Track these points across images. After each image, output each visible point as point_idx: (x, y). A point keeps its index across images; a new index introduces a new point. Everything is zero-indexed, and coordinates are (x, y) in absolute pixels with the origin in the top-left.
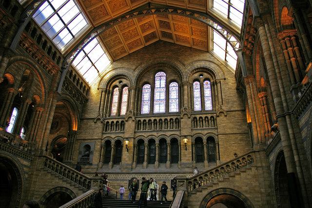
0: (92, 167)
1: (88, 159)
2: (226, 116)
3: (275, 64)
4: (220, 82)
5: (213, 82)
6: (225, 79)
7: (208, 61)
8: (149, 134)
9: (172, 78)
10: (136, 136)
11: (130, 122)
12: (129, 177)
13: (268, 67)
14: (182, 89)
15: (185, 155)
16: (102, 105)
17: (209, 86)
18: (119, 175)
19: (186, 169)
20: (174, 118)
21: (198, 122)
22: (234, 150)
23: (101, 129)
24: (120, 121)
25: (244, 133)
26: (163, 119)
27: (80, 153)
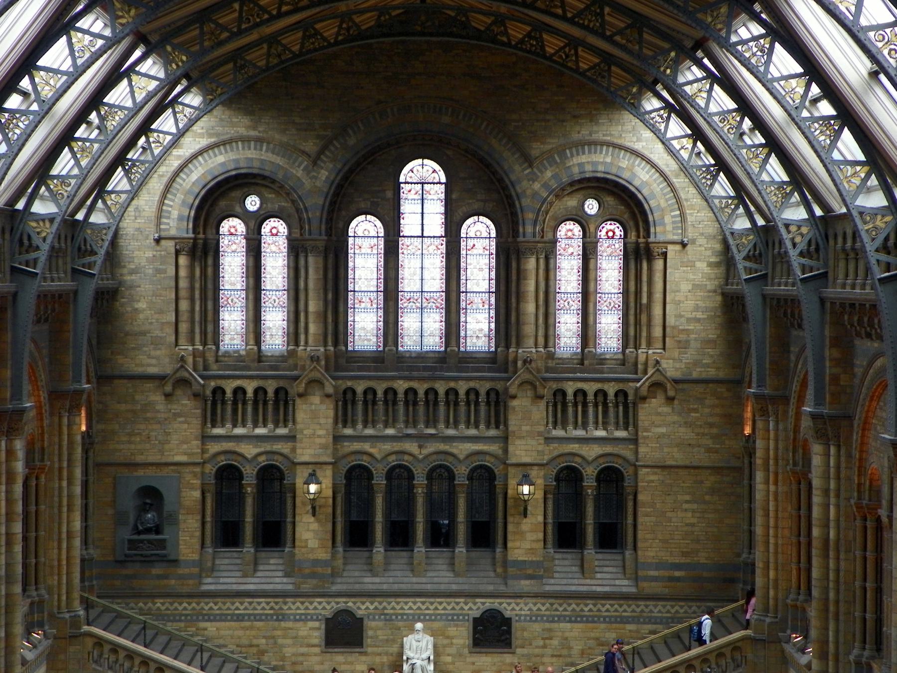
0: (180, 571)
1: (162, 544)
2: (670, 400)
3: (832, 576)
4: (665, 255)
5: (637, 243)
6: (684, 245)
7: (627, 149)
8: (387, 447)
9: (476, 206)
10: (340, 453)
11: (316, 399)
12: (327, 607)
13: (815, 573)
14: (514, 265)
15: (522, 534)
16: (184, 317)
17: (619, 245)
18: (288, 600)
19: (523, 582)
20: (483, 388)
21: (570, 410)
22: (687, 525)
23: (196, 422)
24: (271, 387)
25: (728, 468)
26: (441, 388)
27: (120, 519)
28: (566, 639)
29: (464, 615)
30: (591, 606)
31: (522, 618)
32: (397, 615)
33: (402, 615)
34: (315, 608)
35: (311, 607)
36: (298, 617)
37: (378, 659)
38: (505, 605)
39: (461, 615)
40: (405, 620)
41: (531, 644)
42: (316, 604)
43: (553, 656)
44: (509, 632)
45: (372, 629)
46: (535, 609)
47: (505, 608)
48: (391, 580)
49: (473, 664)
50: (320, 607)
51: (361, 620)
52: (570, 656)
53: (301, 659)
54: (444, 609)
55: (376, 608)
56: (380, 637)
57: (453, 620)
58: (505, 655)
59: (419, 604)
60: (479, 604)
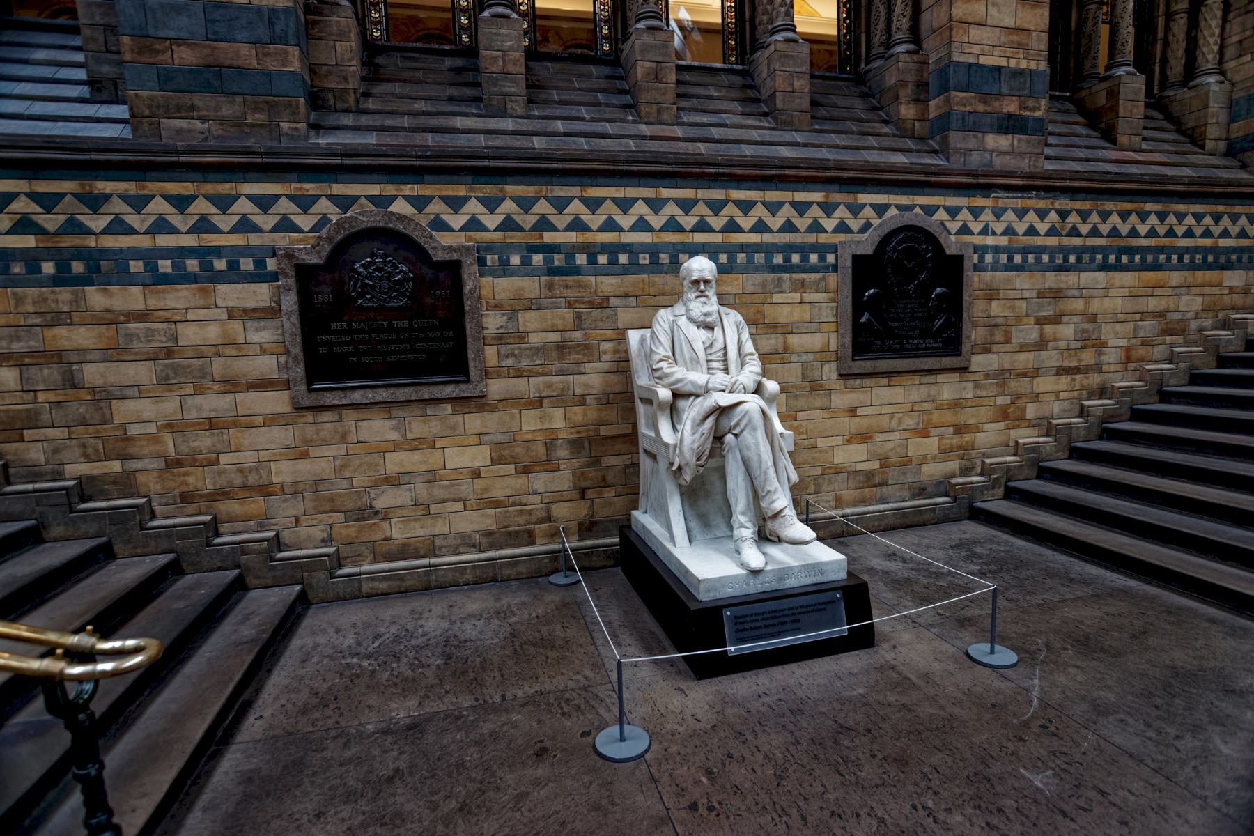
28: (1093, 319)
29: (822, 249)
30: (1153, 220)
31: (989, 258)
32: (591, 251)
33: (613, 249)
34: (245, 226)
35: (224, 222)
36: (165, 266)
37: (530, 422)
38: (941, 215)
39: (815, 248)
40: (625, 271)
41: (1008, 342)
42: (243, 206)
43: (1062, 371)
44: (954, 305)
45: (498, 307)
46: (1021, 228)
47: (942, 223)
48: (560, 126)
49: (852, 412)
50: (267, 221)
51: (454, 268)
52: (1098, 368)
53: (205, 441)
54: (761, 227)
55: (508, 225)
56: (534, 338)
57: (787, 267)
58: (941, 378)
59: (671, 209)
60: (868, 212)
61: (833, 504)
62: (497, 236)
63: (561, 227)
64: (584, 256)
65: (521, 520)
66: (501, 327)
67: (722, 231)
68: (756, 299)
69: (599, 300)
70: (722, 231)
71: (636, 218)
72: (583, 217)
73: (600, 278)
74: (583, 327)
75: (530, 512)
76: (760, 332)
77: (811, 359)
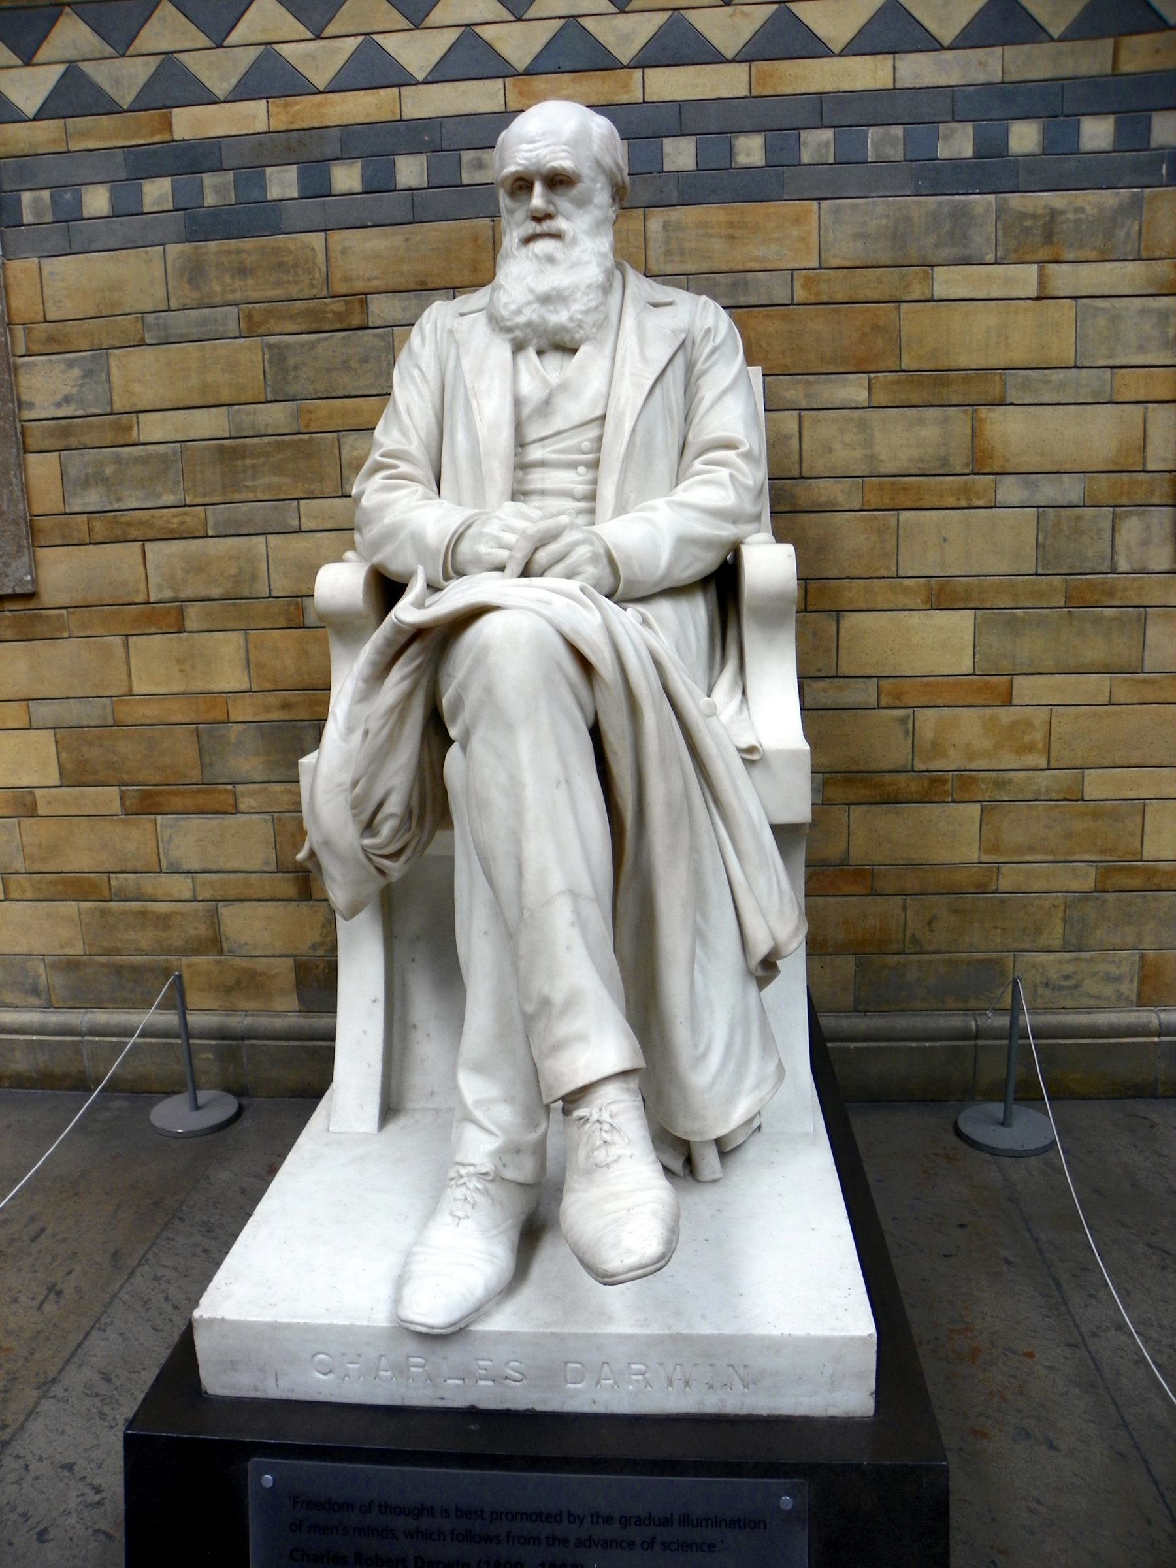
56: (153, 428)
61: (1129, 988)
62: (44, 134)
63: (220, 88)
64: (291, 173)
65: (144, 938)
66: (67, 399)
67: (745, 57)
68: (871, 284)
69: (338, 306)
70: (745, 57)
71: (452, 36)
72: (286, 50)
73: (338, 238)
74: (293, 389)
75: (164, 921)
76: (881, 398)
77: (1074, 496)
